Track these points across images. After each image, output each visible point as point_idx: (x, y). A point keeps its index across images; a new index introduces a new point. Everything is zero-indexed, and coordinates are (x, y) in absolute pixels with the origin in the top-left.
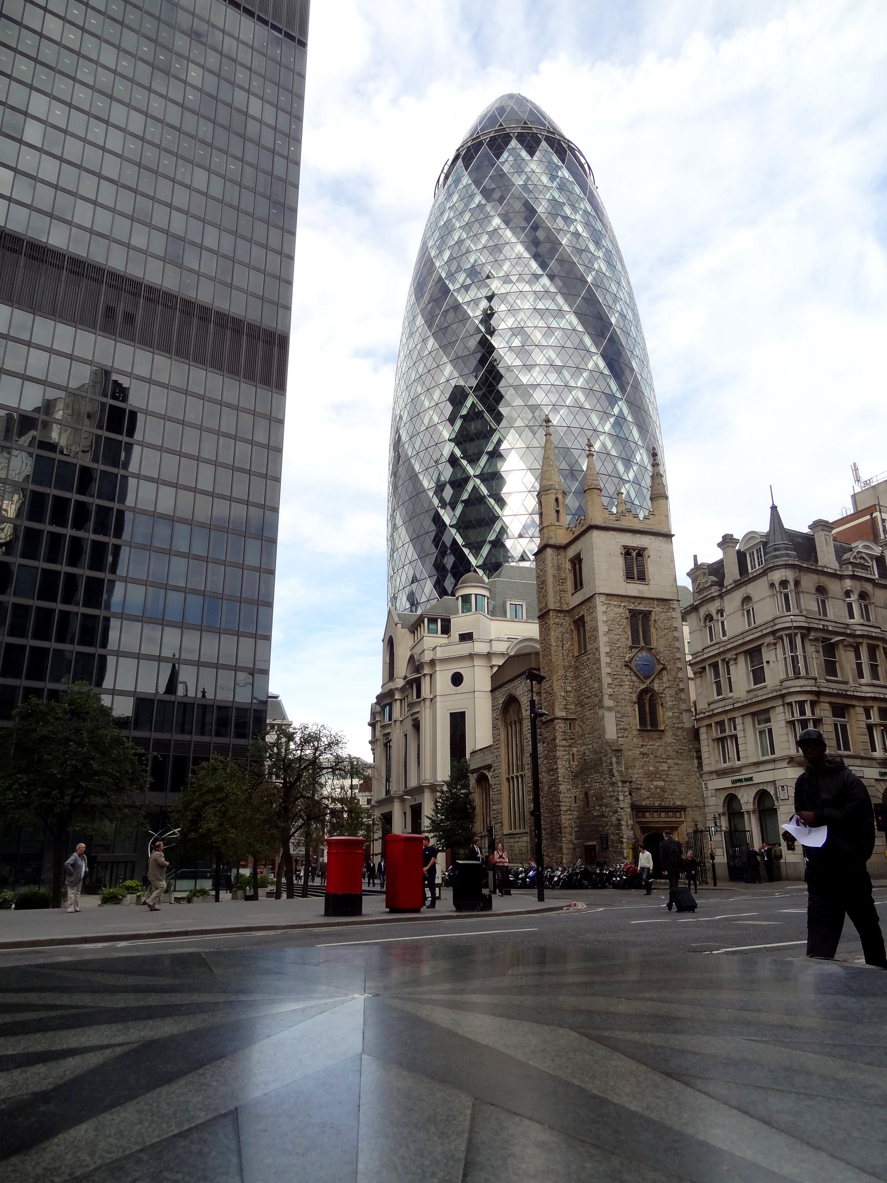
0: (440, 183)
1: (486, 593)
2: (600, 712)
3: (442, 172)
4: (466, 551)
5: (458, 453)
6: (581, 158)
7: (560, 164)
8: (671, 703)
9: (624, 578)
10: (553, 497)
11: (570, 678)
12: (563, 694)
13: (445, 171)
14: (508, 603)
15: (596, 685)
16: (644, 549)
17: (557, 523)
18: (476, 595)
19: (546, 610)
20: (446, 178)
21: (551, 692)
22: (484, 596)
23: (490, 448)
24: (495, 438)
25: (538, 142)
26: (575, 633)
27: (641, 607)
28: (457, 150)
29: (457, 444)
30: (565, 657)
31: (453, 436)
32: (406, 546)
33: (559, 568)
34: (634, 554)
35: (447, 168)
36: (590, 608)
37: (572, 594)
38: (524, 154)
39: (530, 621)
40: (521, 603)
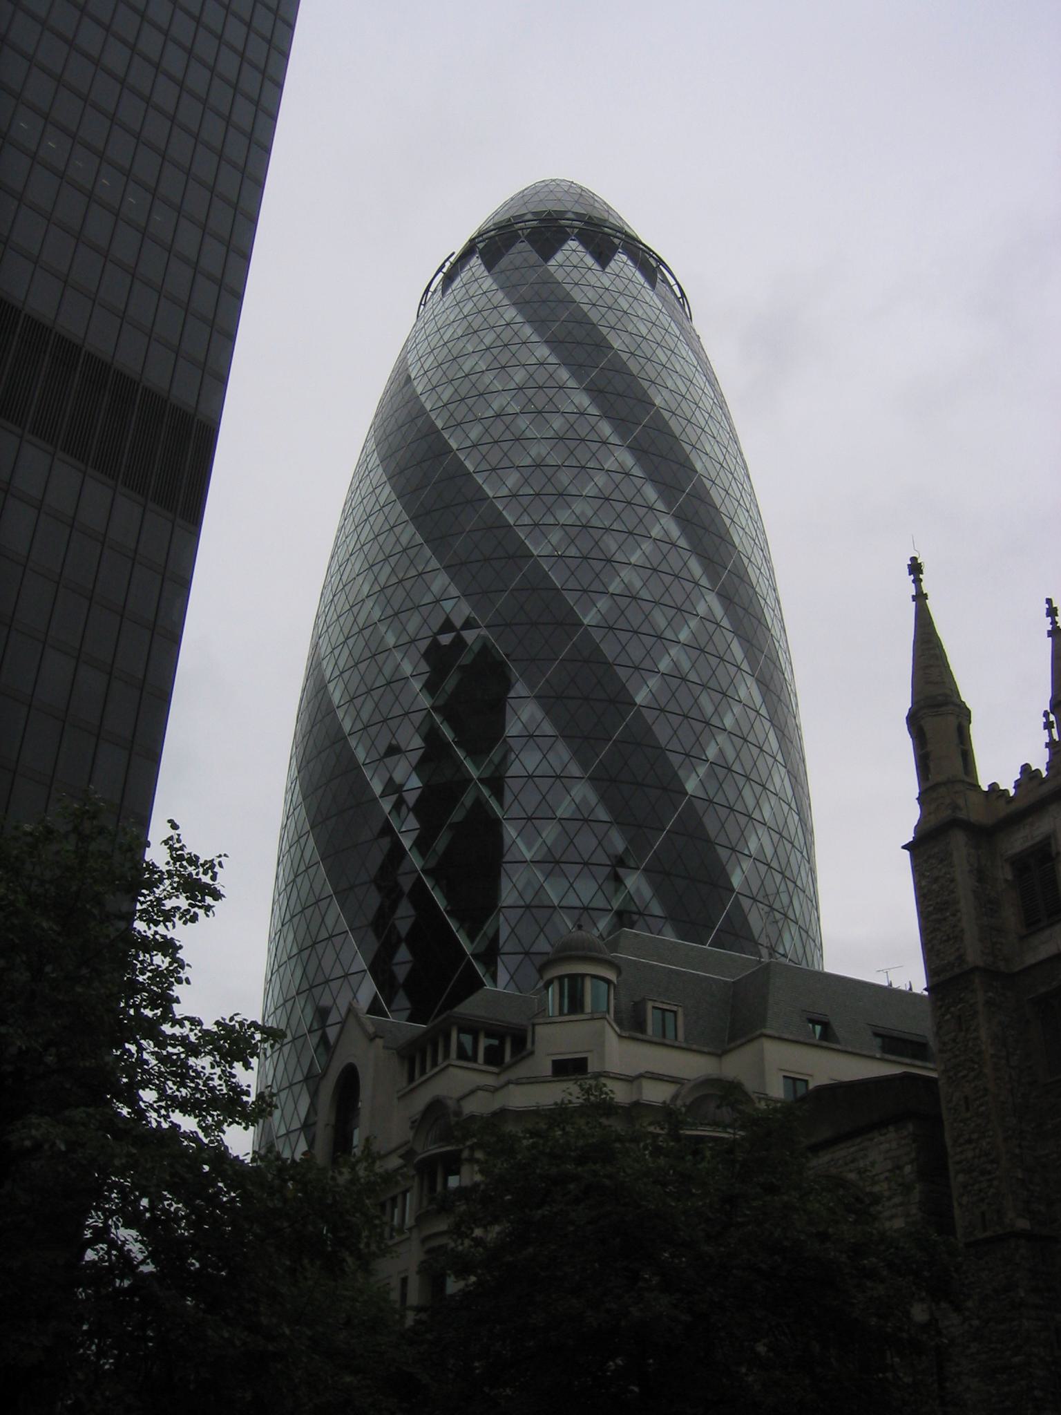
0: (432, 289)
1: (612, 976)
3: (440, 270)
4: (453, 926)
5: (449, 734)
6: (676, 288)
7: (646, 285)
13: (445, 270)
14: (650, 1005)
17: (968, 780)
18: (594, 977)
19: (957, 971)
20: (449, 279)
22: (608, 982)
25: (614, 250)
28: (472, 240)
29: (448, 719)
31: (441, 702)
32: (323, 904)
33: (981, 875)
35: (448, 264)
38: (589, 261)
39: (694, 1047)
40: (675, 1008)
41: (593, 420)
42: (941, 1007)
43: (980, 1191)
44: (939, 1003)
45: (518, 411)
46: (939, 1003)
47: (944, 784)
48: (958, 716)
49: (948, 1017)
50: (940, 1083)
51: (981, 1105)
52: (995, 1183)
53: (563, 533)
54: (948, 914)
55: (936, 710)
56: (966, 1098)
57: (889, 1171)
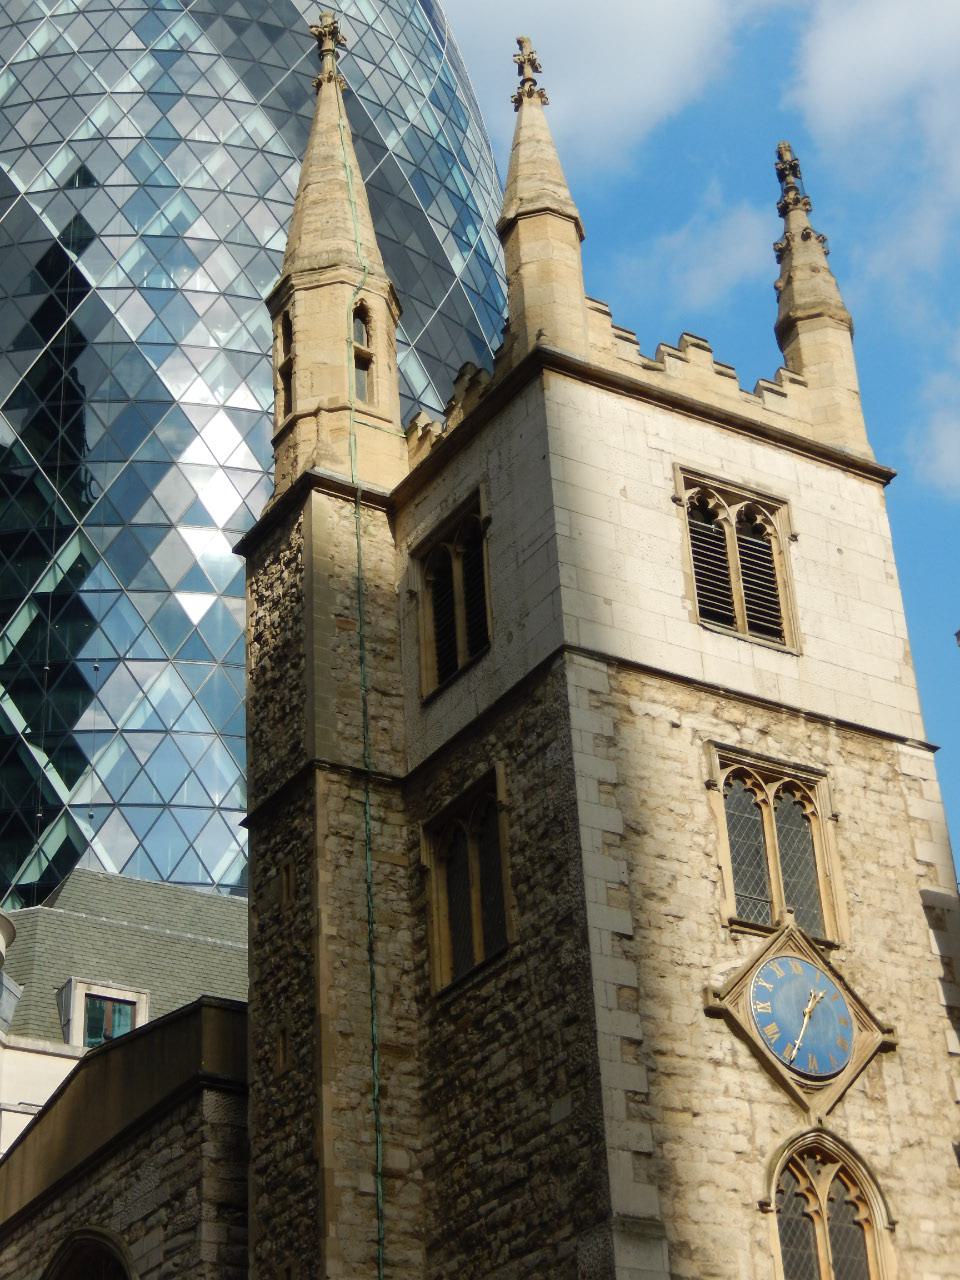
2: (587, 1255)
8: (928, 1226)
9: (692, 605)
10: (348, 299)
11: (402, 1106)
12: (368, 1183)
15: (561, 1109)
16: (774, 504)
17: (363, 407)
19: (290, 775)
21: (303, 1172)
23: (47, 584)
24: (67, 555)
26: (437, 894)
27: (772, 748)
30: (384, 1001)
34: (730, 514)
36: (526, 730)
37: (427, 703)
41: (203, 63)
42: (263, 856)
43: (289, 1223)
44: (262, 848)
45: (76, 49)
46: (262, 848)
47: (315, 413)
48: (359, 289)
49: (273, 872)
50: (250, 1010)
51: (302, 1044)
52: (311, 1203)
53: (143, 250)
54: (288, 665)
55: (316, 277)
56: (283, 1032)
57: (167, 1205)
